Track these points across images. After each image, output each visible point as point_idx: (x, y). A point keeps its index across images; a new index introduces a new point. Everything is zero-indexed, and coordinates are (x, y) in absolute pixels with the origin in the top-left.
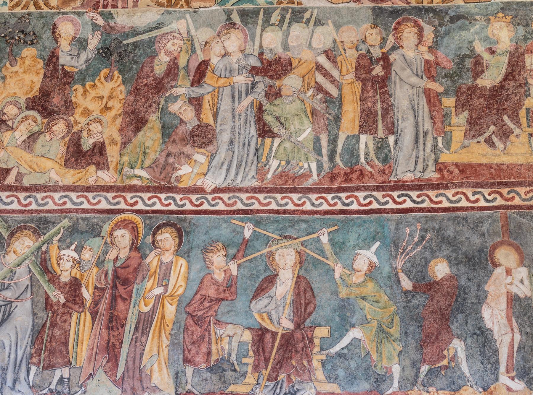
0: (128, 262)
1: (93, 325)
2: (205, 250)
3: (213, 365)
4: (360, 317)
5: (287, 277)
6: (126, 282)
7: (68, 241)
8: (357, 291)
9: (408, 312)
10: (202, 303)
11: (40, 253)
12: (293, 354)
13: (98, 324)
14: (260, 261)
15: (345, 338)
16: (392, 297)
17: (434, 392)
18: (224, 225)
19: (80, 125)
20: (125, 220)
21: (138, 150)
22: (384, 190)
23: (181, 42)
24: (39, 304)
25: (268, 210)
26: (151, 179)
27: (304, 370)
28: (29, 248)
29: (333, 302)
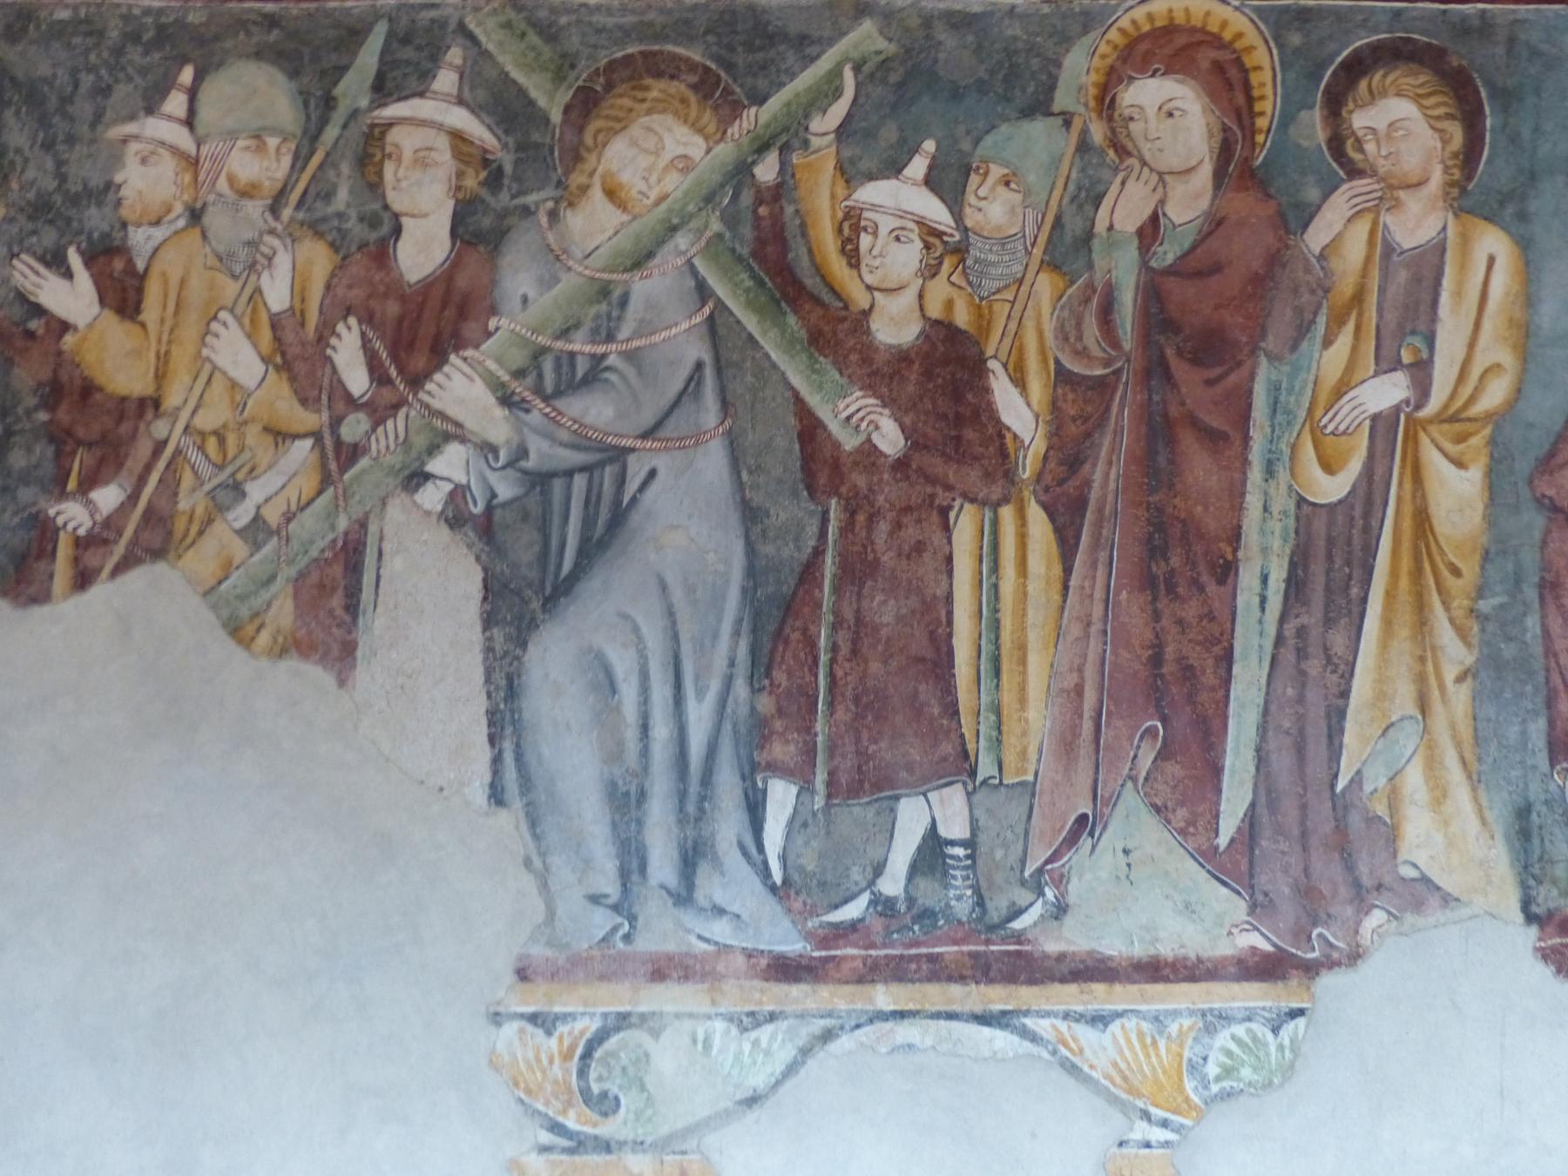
1: (1068, 571)
6: (1217, 350)
7: (889, 133)
11: (747, 198)
28: (685, 171)
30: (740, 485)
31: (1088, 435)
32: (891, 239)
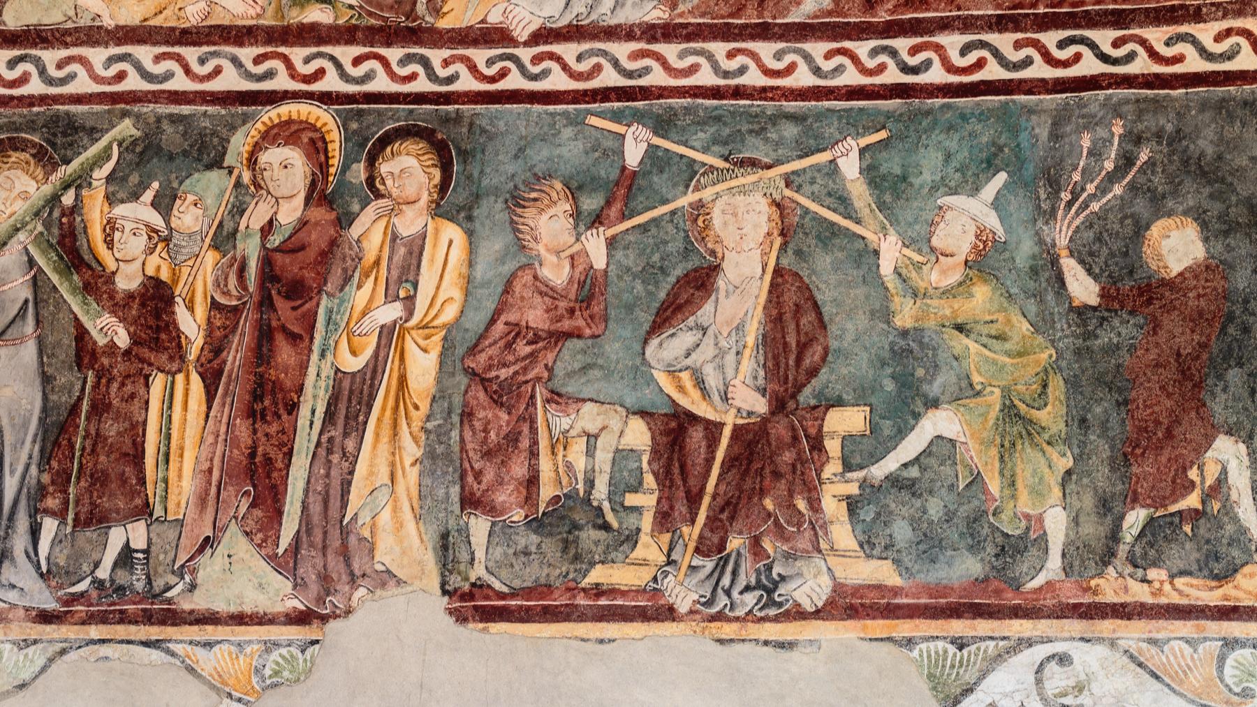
0: (301, 235)
1: (209, 408)
2: (516, 201)
3: (544, 514)
4: (954, 379)
5: (747, 271)
6: (298, 291)
7: (134, 179)
8: (945, 309)
9: (1087, 363)
10: (509, 346)
11: (56, 214)
12: (767, 482)
13: (224, 405)
14: (670, 228)
15: (912, 437)
16: (1042, 325)
17: (1162, 582)
18: (568, 132)
20: (289, 122)
22: (1017, 29)
24: (58, 351)
25: (691, 87)
26: (361, 7)
27: (799, 525)
29: (876, 339)
30: (42, 364)
31: (226, 336)
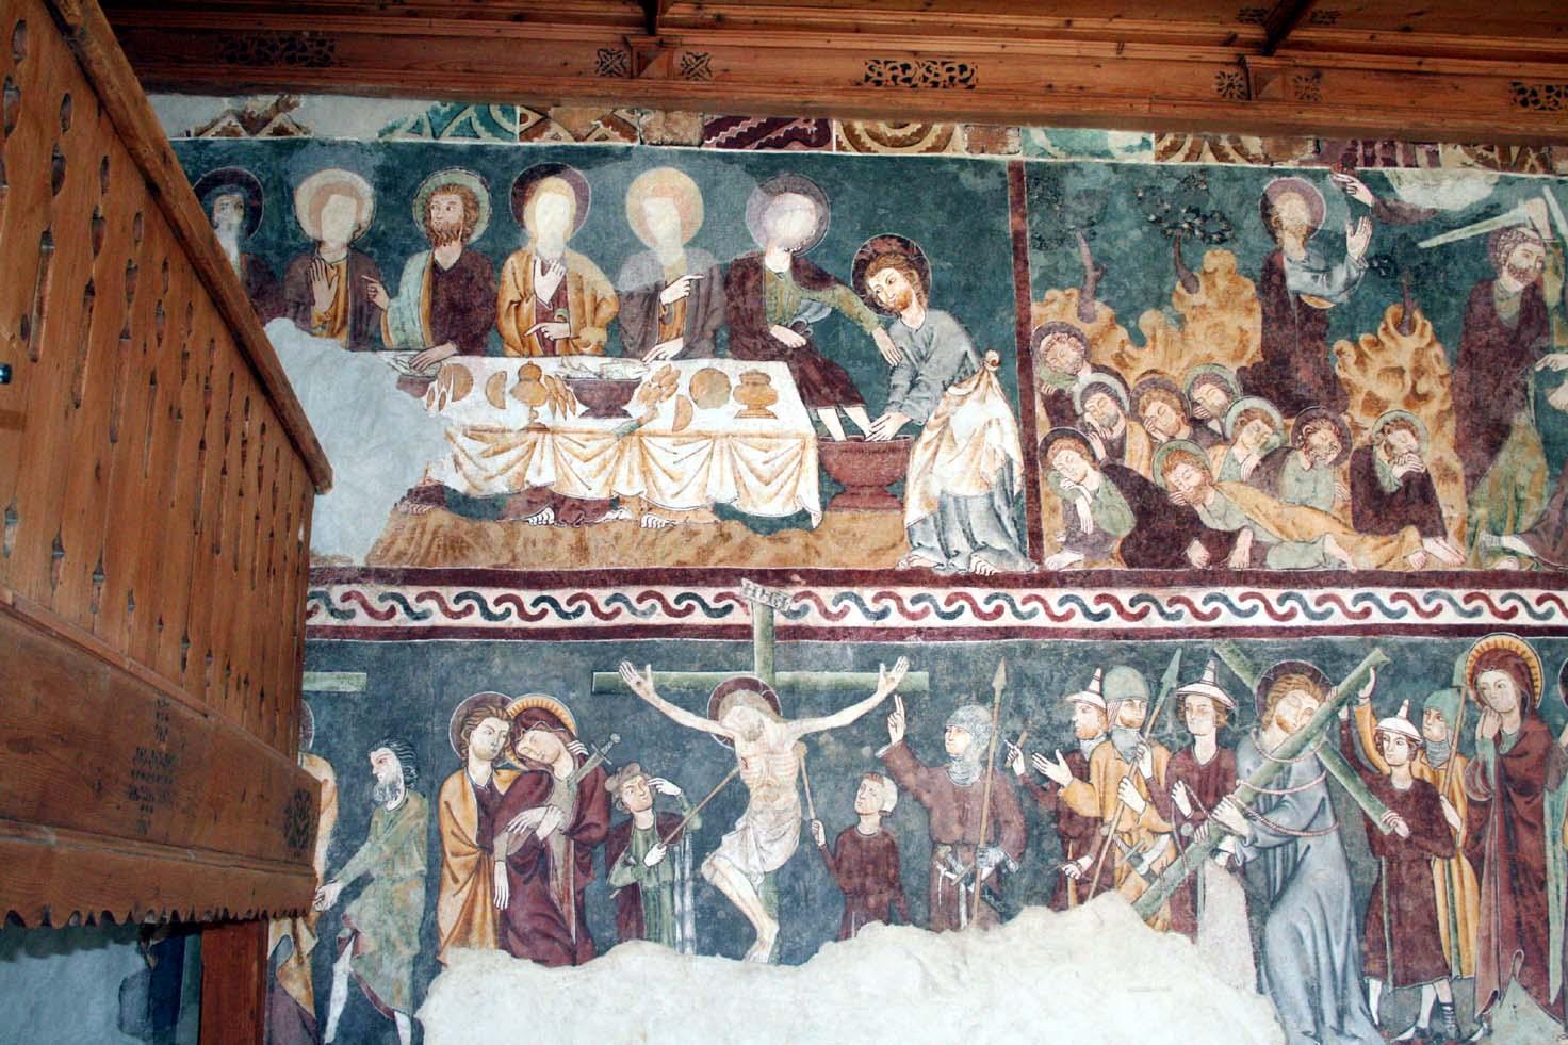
7: (1391, 697)
11: (1336, 728)
19: (1366, 434)
20: (1496, 650)
21: (1503, 492)
23: (1539, 250)
30: (1345, 852)
32: (1396, 743)
